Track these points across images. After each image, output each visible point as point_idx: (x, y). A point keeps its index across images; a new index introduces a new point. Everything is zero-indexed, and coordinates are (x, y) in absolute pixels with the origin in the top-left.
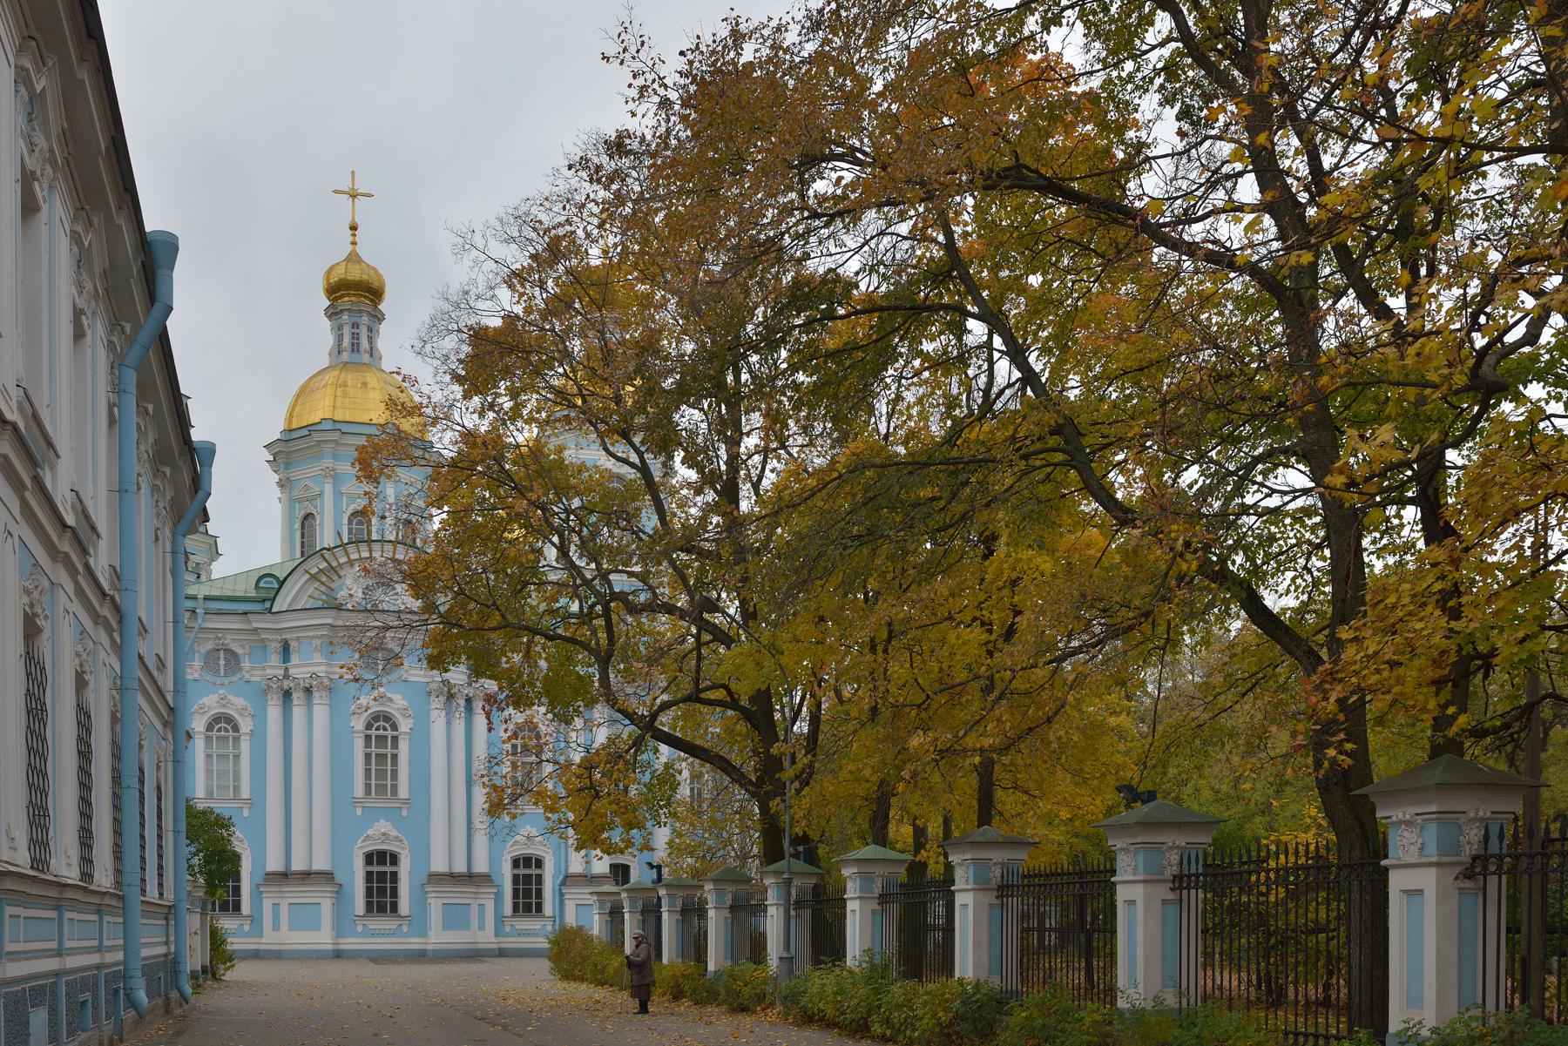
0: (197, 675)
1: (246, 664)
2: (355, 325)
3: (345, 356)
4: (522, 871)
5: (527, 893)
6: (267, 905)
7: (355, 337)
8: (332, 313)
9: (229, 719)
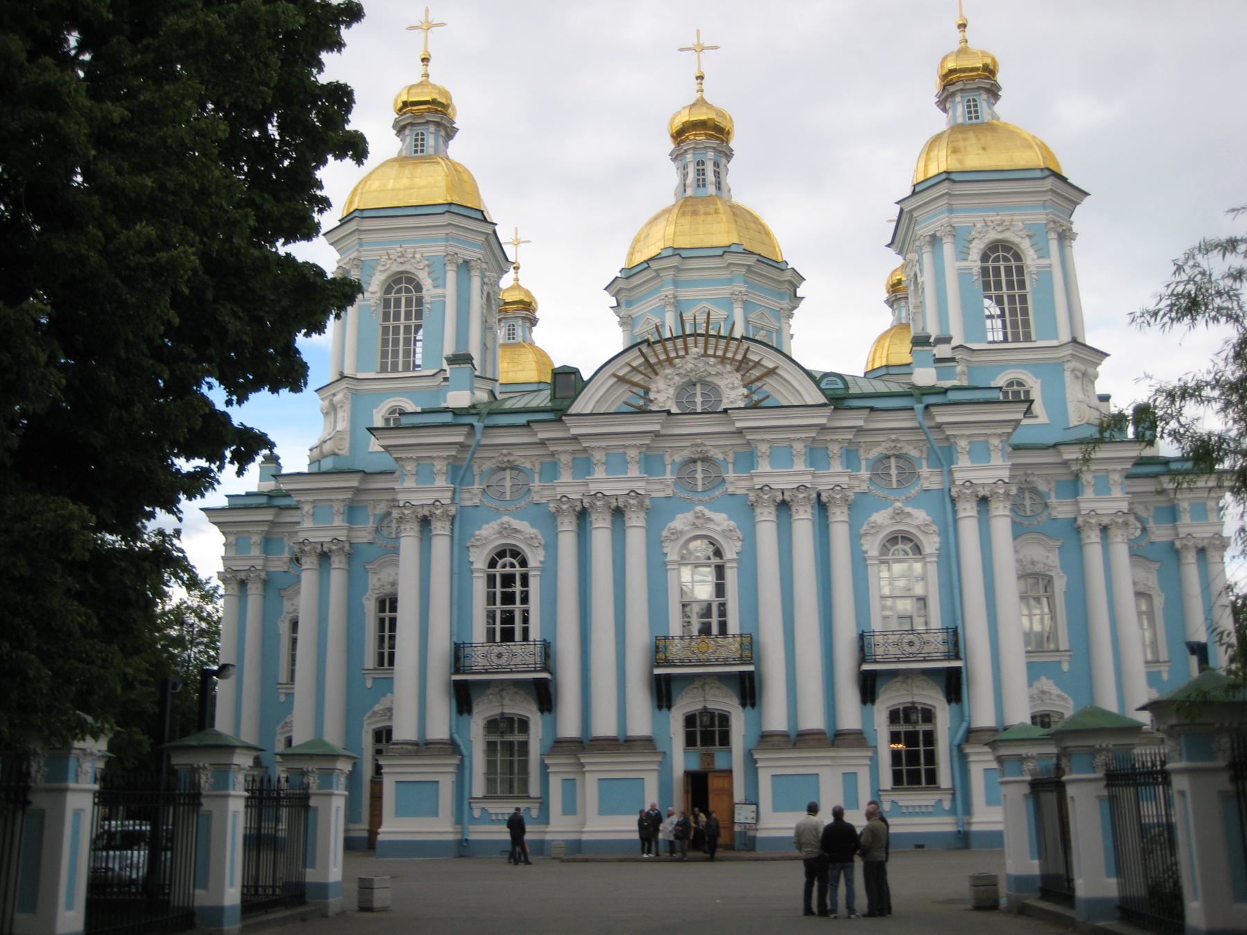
0: (476, 501)
1: (536, 484)
2: (701, 163)
3: (689, 192)
4: (902, 728)
5: (913, 757)
6: (555, 784)
7: (701, 173)
8: (676, 156)
9: (515, 553)
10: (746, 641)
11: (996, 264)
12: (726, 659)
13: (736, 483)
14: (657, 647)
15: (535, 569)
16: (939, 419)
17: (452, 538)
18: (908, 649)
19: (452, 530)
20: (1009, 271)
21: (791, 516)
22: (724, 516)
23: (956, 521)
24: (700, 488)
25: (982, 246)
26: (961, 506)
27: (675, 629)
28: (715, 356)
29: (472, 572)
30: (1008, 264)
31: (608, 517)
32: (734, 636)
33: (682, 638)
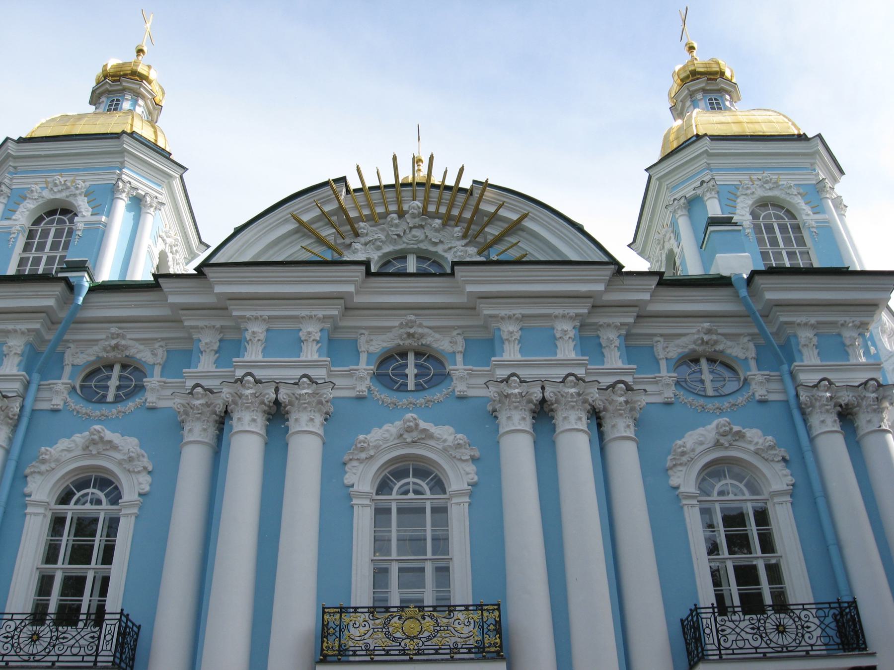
0: (57, 402)
1: (153, 381)
10: (490, 617)
11: (768, 222)
12: (454, 650)
13: (466, 379)
14: (325, 626)
15: (130, 505)
16: (769, 296)
17: (8, 452)
18: (774, 636)
19: (11, 440)
20: (783, 229)
21: (554, 428)
22: (452, 430)
23: (812, 440)
24: (411, 386)
25: (750, 202)
26: (815, 420)
27: (362, 594)
28: (436, 215)
29: (25, 506)
30: (781, 222)
31: (261, 420)
32: (467, 607)
33: (372, 610)
